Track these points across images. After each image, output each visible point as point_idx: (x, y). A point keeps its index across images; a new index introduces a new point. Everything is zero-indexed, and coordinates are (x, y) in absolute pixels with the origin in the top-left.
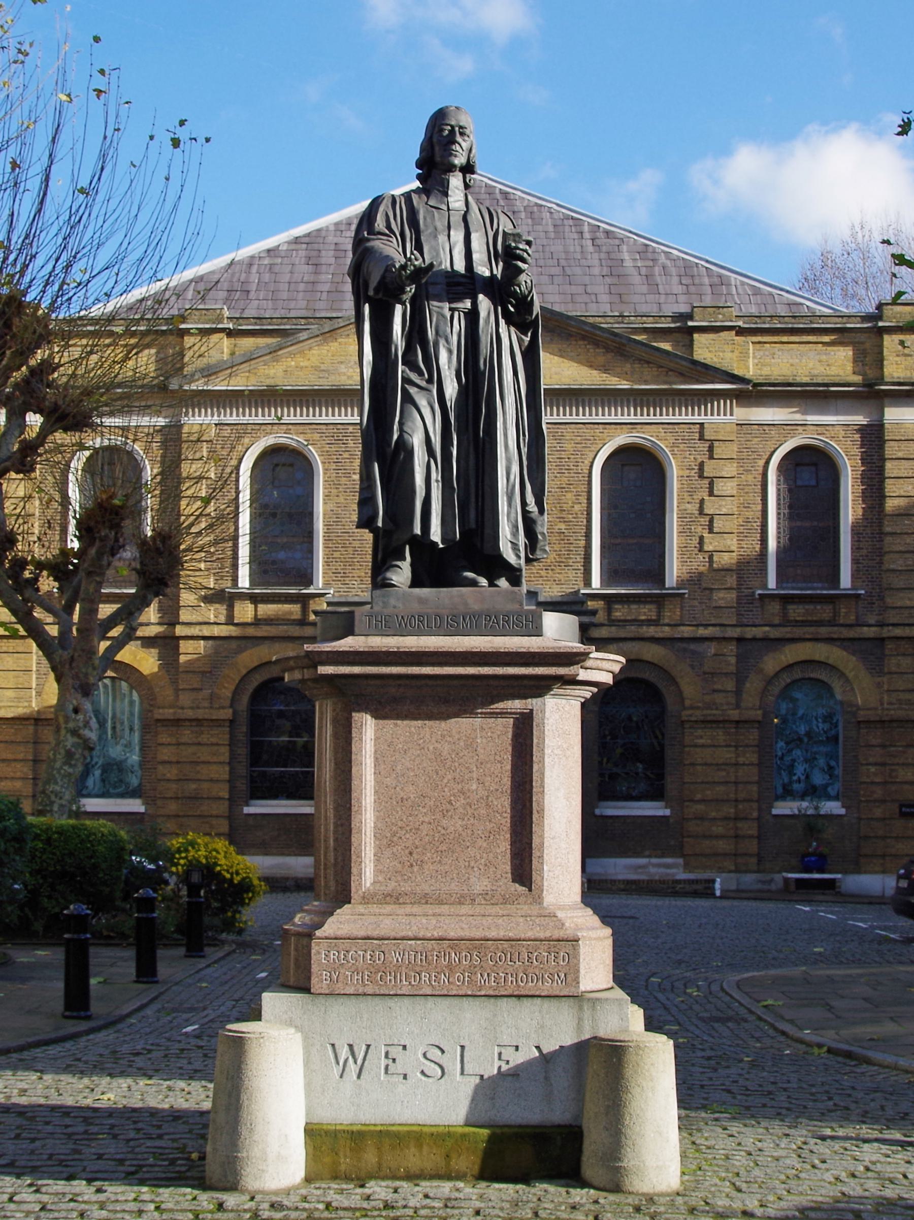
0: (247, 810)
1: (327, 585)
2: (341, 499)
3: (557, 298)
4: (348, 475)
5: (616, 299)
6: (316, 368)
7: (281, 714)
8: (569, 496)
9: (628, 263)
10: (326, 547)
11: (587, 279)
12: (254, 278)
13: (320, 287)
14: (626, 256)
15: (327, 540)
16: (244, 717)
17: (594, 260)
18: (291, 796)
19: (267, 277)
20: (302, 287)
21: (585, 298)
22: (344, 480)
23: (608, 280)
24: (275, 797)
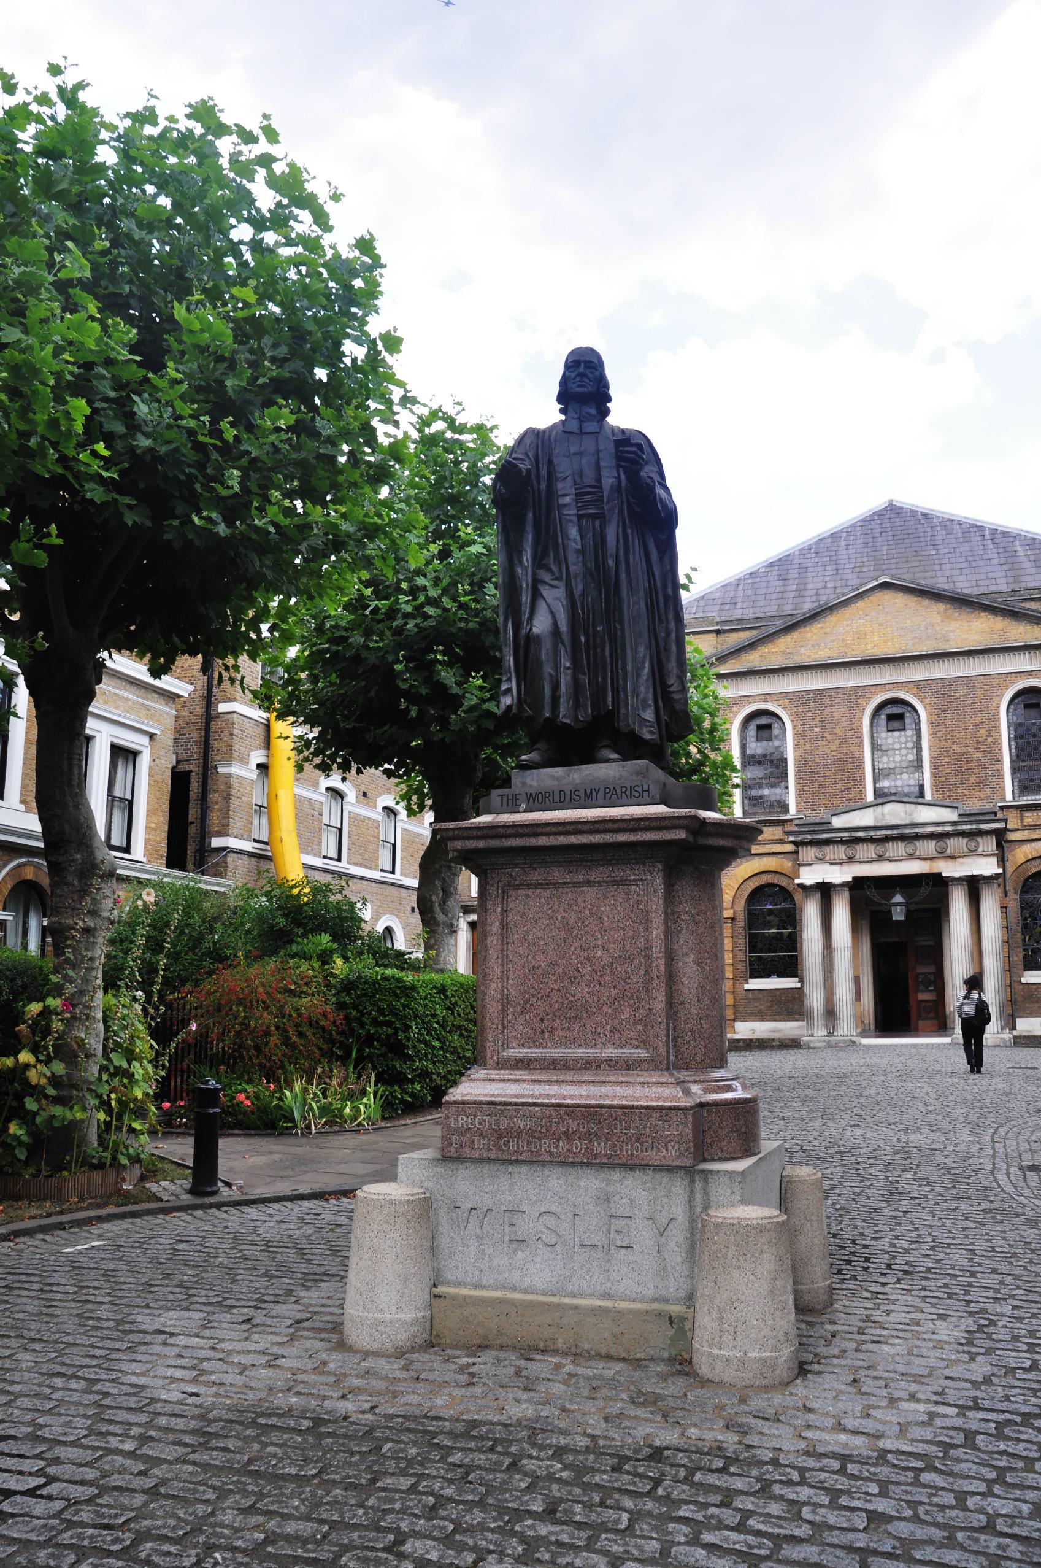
0: (746, 987)
1: (799, 811)
2: (808, 746)
3: (965, 584)
4: (811, 729)
5: (1011, 580)
6: (784, 652)
7: (770, 912)
8: (982, 731)
9: (1021, 553)
10: (797, 783)
11: (989, 569)
12: (740, 593)
13: (787, 595)
14: (1019, 548)
15: (798, 778)
16: (741, 917)
17: (993, 554)
18: (781, 975)
19: (749, 592)
20: (775, 596)
21: (987, 582)
22: (808, 733)
23: (1005, 567)
24: (769, 976)
